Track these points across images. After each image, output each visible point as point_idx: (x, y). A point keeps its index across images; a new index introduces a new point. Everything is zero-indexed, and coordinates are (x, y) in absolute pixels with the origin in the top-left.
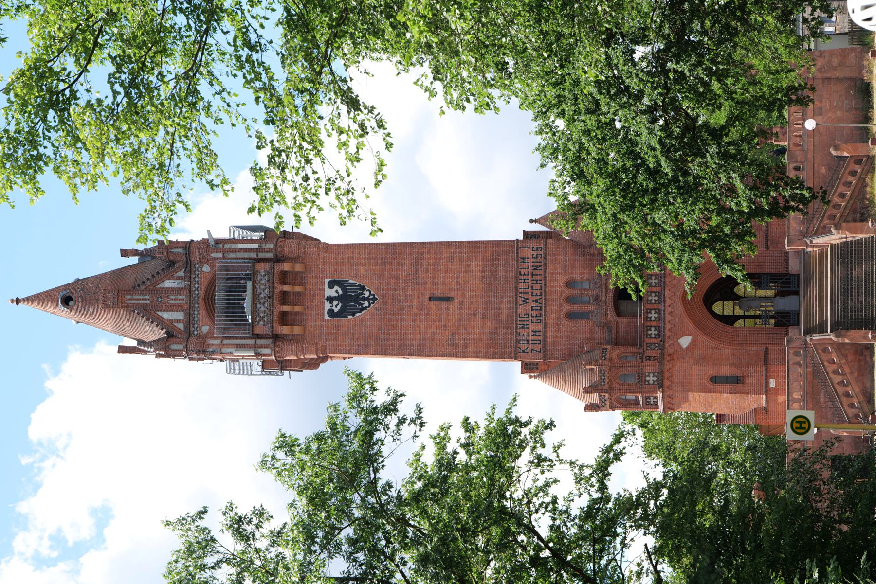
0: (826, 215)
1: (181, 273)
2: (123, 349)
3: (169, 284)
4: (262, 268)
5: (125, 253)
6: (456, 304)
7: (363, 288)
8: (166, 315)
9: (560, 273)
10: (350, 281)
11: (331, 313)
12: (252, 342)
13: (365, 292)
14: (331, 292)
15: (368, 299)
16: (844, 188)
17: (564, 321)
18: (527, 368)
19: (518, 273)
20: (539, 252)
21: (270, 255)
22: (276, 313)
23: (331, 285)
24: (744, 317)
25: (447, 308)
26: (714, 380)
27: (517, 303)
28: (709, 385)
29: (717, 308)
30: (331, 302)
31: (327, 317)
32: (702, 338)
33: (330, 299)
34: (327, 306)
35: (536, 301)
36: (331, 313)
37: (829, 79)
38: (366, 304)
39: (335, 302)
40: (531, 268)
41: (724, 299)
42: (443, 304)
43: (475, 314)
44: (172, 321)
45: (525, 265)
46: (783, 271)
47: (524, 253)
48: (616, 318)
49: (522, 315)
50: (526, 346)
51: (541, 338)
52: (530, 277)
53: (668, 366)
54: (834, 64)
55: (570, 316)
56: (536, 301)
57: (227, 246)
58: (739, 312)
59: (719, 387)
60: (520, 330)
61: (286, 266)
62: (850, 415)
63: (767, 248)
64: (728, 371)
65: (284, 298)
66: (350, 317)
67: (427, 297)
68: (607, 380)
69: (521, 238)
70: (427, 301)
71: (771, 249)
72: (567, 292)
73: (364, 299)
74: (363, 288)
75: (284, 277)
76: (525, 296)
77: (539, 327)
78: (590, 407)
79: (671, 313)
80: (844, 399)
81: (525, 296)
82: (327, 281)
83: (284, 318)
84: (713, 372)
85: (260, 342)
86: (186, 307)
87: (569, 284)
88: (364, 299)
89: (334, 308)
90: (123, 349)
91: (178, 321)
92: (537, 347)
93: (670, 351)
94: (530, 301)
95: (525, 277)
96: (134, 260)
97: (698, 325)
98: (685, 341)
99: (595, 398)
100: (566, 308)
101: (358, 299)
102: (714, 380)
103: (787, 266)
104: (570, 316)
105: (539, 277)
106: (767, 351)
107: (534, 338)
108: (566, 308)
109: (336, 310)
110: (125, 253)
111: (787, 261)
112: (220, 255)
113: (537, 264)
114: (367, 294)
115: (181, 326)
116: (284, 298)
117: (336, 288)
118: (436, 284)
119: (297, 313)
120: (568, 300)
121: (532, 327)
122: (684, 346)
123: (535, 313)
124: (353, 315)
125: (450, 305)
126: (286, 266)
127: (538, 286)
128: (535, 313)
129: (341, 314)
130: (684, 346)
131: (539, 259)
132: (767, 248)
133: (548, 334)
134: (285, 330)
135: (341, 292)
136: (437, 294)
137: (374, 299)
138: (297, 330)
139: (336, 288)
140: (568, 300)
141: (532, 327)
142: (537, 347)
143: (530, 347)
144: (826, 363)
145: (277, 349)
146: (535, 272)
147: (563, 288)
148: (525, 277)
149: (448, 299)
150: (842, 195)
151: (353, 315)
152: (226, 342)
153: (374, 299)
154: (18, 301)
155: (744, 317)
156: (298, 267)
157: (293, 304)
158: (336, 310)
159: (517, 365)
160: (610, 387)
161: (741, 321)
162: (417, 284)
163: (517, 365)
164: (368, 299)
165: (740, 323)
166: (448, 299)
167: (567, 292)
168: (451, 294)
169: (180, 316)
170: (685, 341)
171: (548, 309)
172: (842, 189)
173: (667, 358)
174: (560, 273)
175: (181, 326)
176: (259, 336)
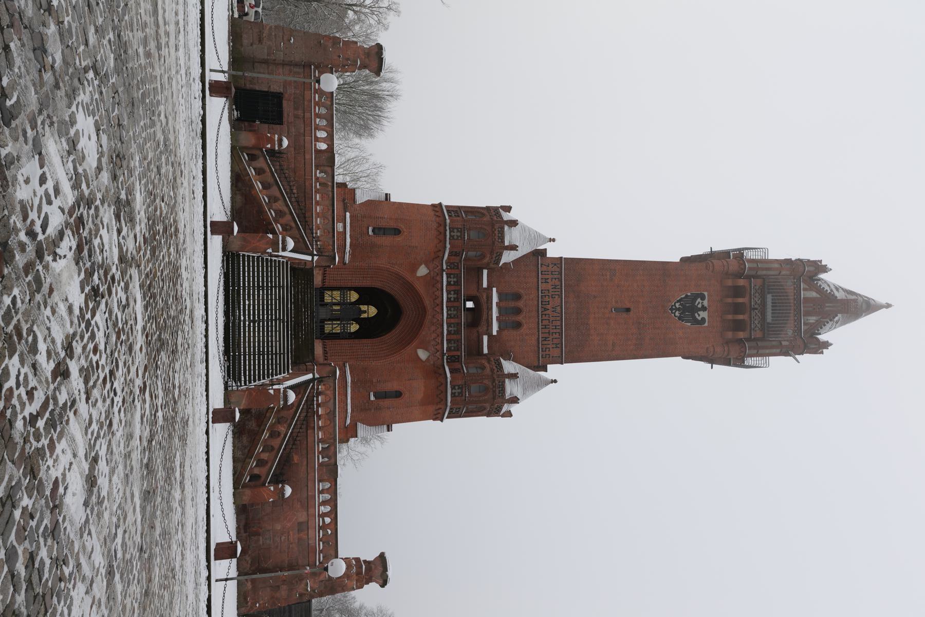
4: (759, 334)
7: (680, 318)
8: (814, 294)
9: (527, 335)
11: (703, 298)
12: (760, 273)
14: (703, 314)
15: (677, 309)
16: (273, 444)
17: (522, 291)
22: (748, 296)
23: (703, 319)
25: (616, 302)
26: (397, 232)
28: (402, 226)
29: (372, 311)
30: (703, 306)
31: (706, 294)
33: (704, 309)
34: (706, 303)
35: (546, 309)
37: (291, 567)
38: (677, 305)
39: (700, 306)
41: (368, 319)
43: (595, 297)
44: (811, 290)
45: (556, 341)
54: (285, 587)
55: (518, 297)
56: (546, 309)
57: (778, 351)
59: (392, 224)
62: (261, 159)
64: (386, 241)
65: (737, 309)
67: (631, 313)
68: (496, 232)
69: (549, 366)
72: (520, 318)
73: (679, 309)
74: (680, 318)
75: (738, 326)
76: (556, 314)
78: (508, 209)
80: (271, 180)
81: (556, 314)
82: (706, 324)
83: (737, 292)
84: (398, 239)
87: (518, 325)
88: (679, 309)
97: (409, 288)
99: (506, 216)
100: (520, 304)
101: (683, 310)
102: (397, 232)
103: (324, 347)
104: (518, 297)
107: (547, 277)
108: (520, 304)
109: (699, 300)
111: (325, 352)
112: (784, 343)
114: (677, 314)
116: (737, 309)
117: (699, 318)
120: (518, 311)
122: (423, 266)
123: (547, 299)
124: (687, 296)
129: (696, 296)
130: (423, 266)
133: (536, 280)
134: (741, 282)
136: (624, 315)
138: (730, 283)
139: (699, 318)
140: (518, 311)
144: (293, 225)
146: (547, 335)
147: (524, 321)
151: (687, 296)
152: (776, 272)
154: (888, 306)
156: (730, 335)
158: (699, 300)
159: (548, 255)
160: (493, 226)
161: (353, 300)
164: (677, 309)
165: (354, 296)
167: (520, 318)
171: (536, 303)
174: (527, 335)
176: (756, 277)
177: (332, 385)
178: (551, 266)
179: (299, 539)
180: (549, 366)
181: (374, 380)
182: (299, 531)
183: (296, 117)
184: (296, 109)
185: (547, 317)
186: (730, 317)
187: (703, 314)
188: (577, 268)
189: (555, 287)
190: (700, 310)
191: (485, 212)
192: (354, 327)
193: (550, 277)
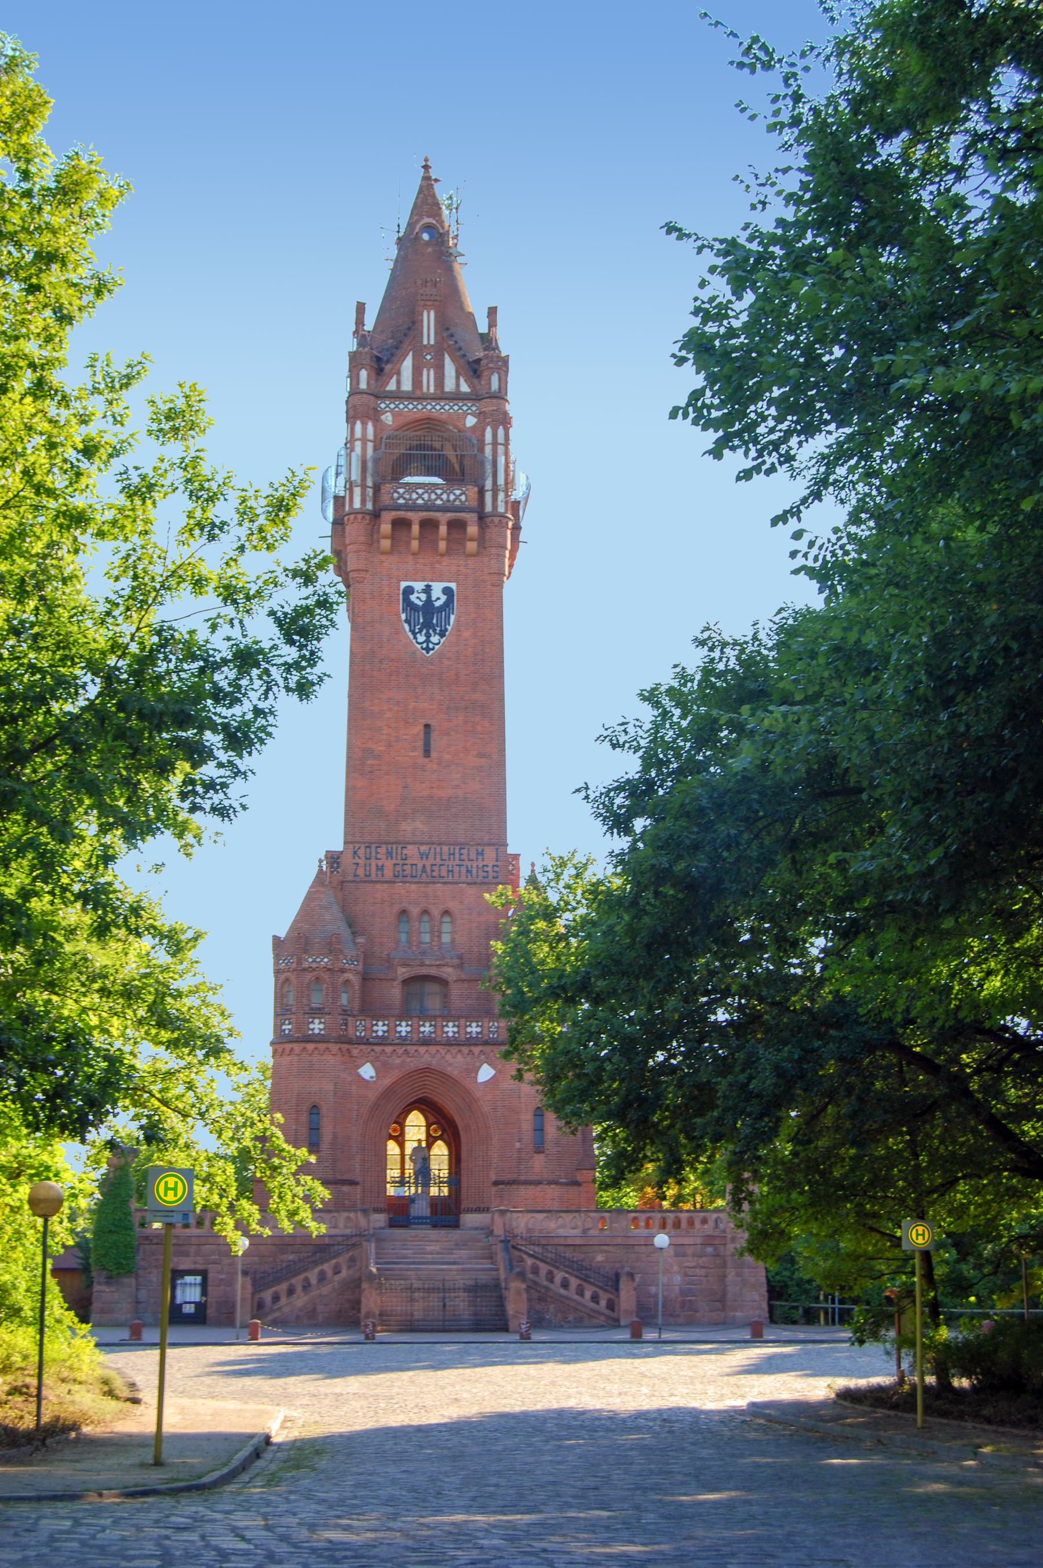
0: (538, 1263)
1: (465, 388)
2: (361, 308)
3: (450, 368)
5: (492, 312)
6: (422, 761)
7: (442, 634)
10: (452, 617)
13: (437, 637)
14: (437, 589)
15: (428, 641)
18: (333, 859)
19: (462, 846)
20: (491, 874)
21: (489, 508)
22: (409, 515)
23: (447, 591)
24: (403, 1155)
25: (414, 749)
27: (422, 844)
31: (404, 584)
32: (372, 1096)
33: (428, 590)
34: (419, 586)
36: (409, 591)
38: (421, 638)
39: (424, 597)
40: (469, 864)
42: (420, 744)
44: (399, 373)
45: (473, 856)
46: (464, 1205)
47: (490, 853)
48: (400, 979)
49: (405, 851)
50: (362, 856)
51: (373, 877)
52: (458, 862)
53: (334, 1048)
58: (409, 1147)
59: (304, 1117)
60: (384, 847)
61: (472, 530)
63: (496, 1183)
65: (429, 525)
66: (403, 616)
69: (510, 850)
70: (424, 721)
71: (494, 1189)
73: (428, 636)
75: (457, 526)
76: (432, 855)
77: (388, 873)
79: (406, 1052)
81: (432, 855)
82: (453, 585)
84: (324, 1111)
85: (370, 492)
86: (418, 393)
88: (428, 636)
89: (416, 595)
90: (361, 308)
91: (399, 382)
92: (361, 871)
93: (355, 1052)
94: (424, 862)
95: (457, 856)
96: (483, 327)
98: (367, 1071)
105: (456, 875)
106: (353, 1183)
107: (374, 868)
109: (413, 598)
110: (492, 312)
111: (478, 1210)
113: (474, 872)
114: (435, 639)
115: (392, 386)
116: (429, 525)
117: (444, 598)
118: (448, 734)
119: (409, 543)
121: (389, 864)
124: (407, 621)
125: (419, 753)
126: (472, 530)
127: (444, 873)
128: (407, 868)
129: (409, 605)
131: (481, 873)
132: (496, 1183)
133: (379, 886)
134: (386, 528)
135: (437, 604)
136: (434, 735)
137: (428, 649)
138: (386, 544)
139: (444, 598)
141: (389, 864)
142: (361, 871)
143: (361, 862)
145: (360, 516)
146: (463, 870)
147: (442, 907)
148: (457, 856)
149: (427, 753)
150: (565, 1285)
151: (407, 621)
153: (428, 649)
154: (426, 167)
155: (403, 1155)
156: (472, 546)
157: (421, 537)
158: (413, 598)
159: (338, 846)
162: (448, 708)
163: (338, 846)
164: (428, 641)
166: (427, 753)
168: (434, 754)
169: (407, 386)
170: (367, 1071)
171: (414, 887)
172: (574, 1282)
173: (345, 1046)
175: (392, 386)
177: (515, 1215)
178: (357, 860)
179: (694, 1255)
180: (510, 850)
181: (518, 1145)
182: (684, 1255)
183: (198, 1253)
184: (187, 1255)
185: (436, 868)
186: (442, 545)
187: (437, 590)
188: (358, 810)
189: (389, 854)
190: (429, 597)
191: (283, 977)
192: (440, 1150)
193: (373, 863)
